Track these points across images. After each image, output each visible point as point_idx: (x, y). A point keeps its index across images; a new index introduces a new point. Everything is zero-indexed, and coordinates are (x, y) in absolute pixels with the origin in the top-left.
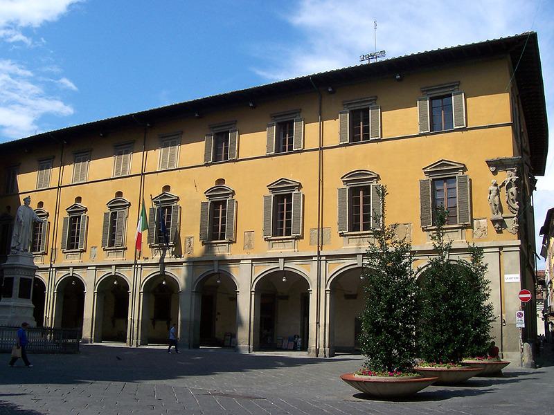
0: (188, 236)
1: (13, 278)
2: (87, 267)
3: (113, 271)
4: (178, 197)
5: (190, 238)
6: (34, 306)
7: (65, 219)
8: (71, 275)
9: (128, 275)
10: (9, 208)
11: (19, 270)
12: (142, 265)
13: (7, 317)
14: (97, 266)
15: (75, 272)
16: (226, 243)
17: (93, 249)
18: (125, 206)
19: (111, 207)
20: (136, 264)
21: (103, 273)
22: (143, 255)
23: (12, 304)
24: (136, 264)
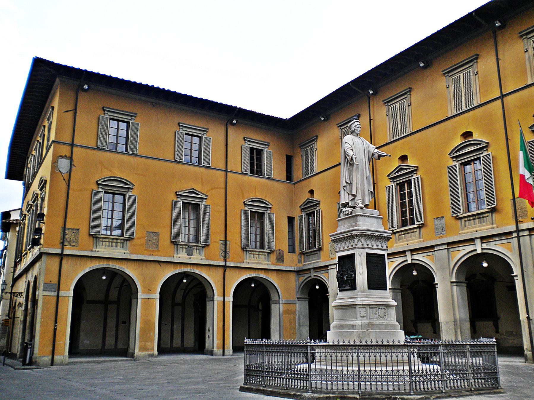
2: (432, 247)
3: (478, 248)
6: (396, 304)
7: (389, 189)
8: (409, 261)
10: (311, 192)
13: (353, 326)
14: (448, 244)
15: (415, 257)
17: (437, 222)
20: (518, 231)
21: (462, 253)
23: (358, 301)
24: (518, 231)
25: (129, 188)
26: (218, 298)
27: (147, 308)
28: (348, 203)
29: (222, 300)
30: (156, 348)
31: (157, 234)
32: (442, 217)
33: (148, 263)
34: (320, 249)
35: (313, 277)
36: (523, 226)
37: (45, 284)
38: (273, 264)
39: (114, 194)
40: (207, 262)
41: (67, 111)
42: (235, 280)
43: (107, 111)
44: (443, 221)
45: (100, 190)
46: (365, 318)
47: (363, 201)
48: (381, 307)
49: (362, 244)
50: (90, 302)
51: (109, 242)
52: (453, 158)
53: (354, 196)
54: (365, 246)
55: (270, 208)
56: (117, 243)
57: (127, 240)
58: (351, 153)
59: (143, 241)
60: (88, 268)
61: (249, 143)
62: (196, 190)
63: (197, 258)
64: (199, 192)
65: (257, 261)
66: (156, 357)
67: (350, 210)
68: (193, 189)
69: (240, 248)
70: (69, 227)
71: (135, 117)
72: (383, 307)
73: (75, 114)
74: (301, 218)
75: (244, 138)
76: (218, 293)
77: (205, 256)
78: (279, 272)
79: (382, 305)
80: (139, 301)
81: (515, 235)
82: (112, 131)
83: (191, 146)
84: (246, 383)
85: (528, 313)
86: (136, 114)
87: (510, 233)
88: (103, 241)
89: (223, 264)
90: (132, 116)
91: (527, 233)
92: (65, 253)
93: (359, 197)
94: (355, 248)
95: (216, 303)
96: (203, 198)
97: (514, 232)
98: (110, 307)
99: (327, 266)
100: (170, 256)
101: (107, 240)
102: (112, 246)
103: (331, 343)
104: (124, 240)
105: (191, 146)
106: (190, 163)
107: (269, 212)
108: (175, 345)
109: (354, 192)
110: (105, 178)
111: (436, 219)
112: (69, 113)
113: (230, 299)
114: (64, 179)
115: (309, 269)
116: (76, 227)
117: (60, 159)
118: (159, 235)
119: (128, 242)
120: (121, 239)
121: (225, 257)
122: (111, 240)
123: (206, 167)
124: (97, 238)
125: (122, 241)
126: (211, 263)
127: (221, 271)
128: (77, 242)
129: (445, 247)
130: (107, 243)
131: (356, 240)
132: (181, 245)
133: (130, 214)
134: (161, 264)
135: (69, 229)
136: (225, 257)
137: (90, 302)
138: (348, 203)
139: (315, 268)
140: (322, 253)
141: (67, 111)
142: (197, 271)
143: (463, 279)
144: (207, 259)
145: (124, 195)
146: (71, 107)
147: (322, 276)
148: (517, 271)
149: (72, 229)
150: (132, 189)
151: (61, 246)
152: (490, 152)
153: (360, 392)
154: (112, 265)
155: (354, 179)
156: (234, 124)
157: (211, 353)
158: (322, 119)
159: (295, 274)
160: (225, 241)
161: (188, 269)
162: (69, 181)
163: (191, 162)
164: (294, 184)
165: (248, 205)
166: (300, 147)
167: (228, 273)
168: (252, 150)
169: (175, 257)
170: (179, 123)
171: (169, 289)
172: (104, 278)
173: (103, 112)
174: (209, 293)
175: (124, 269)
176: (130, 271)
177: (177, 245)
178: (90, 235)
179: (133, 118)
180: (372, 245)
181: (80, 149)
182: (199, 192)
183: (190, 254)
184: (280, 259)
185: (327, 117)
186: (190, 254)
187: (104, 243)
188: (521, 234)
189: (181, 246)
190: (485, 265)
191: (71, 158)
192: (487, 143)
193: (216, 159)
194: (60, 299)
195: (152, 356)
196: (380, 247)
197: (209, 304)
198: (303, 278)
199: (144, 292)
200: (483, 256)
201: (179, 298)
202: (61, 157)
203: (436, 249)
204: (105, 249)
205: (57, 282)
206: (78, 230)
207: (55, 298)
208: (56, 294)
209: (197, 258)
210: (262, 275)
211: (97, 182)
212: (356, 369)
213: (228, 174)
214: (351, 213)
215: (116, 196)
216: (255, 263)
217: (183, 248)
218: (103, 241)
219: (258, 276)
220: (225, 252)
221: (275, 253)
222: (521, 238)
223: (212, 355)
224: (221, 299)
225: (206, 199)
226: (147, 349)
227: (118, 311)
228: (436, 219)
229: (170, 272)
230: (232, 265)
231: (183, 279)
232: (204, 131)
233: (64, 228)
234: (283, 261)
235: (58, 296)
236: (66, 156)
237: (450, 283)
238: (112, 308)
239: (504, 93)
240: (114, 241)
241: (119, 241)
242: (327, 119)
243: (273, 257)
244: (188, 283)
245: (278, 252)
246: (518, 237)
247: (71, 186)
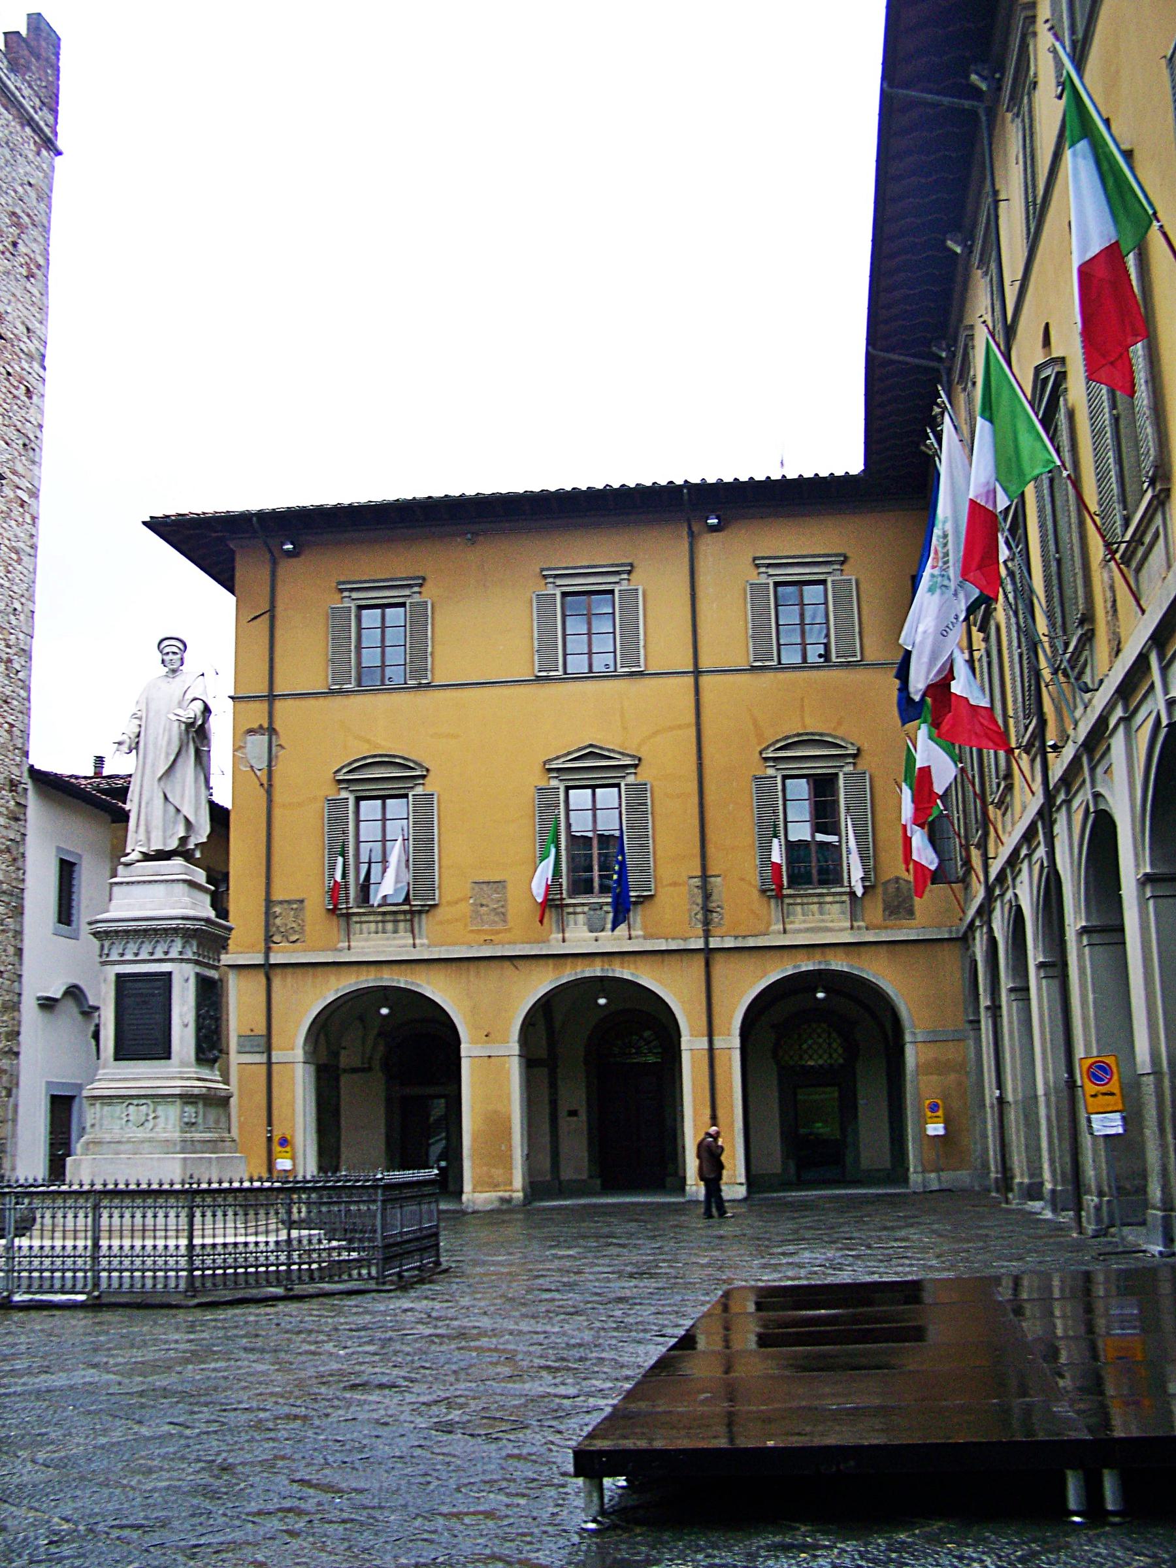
26: (691, 1044)
29: (706, 1046)
37: (240, 1036)
41: (255, 618)
42: (743, 988)
45: (344, 794)
48: (135, 1102)
51: (377, 922)
55: (855, 756)
56: (396, 921)
57: (420, 912)
59: (465, 908)
60: (332, 992)
61: (771, 571)
62: (601, 748)
64: (609, 750)
65: (821, 926)
68: (591, 746)
69: (755, 894)
70: (281, 898)
71: (421, 585)
73: (273, 619)
76: (692, 1028)
77: (644, 928)
78: (898, 948)
79: (139, 1097)
82: (371, 638)
86: (424, 579)
88: (361, 922)
89: (699, 944)
92: (272, 961)
100: (537, 942)
101: (371, 918)
102: (384, 932)
104: (412, 912)
106: (591, 675)
107: (850, 768)
110: (350, 764)
112: (259, 620)
113: (730, 1041)
114: (262, 785)
116: (298, 897)
117: (249, 738)
118: (505, 887)
119: (424, 916)
120: (405, 912)
122: (380, 918)
123: (632, 674)
125: (408, 917)
127: (698, 963)
128: (302, 932)
130: (373, 926)
132: (568, 905)
133: (421, 846)
134: (520, 963)
135: (281, 902)
136: (706, 923)
141: (255, 618)
142: (624, 972)
149: (289, 902)
150: (424, 777)
151: (262, 945)
156: (714, 529)
160: (705, 877)
161: (595, 970)
162: (270, 785)
163: (591, 671)
167: (720, 968)
169: (553, 942)
171: (545, 1028)
175: (418, 985)
176: (436, 989)
179: (416, 589)
181: (290, 702)
182: (609, 750)
187: (365, 926)
189: (571, 910)
191: (272, 731)
193: (665, 643)
194: (275, 1068)
195: (508, 1201)
196: (159, 955)
199: (473, 1042)
202: (251, 731)
204: (366, 940)
205: (264, 1032)
206: (302, 901)
207: (264, 1067)
208: (263, 1058)
210: (839, 964)
212: (183, 1242)
215: (388, 801)
216: (807, 930)
217: (575, 913)
218: (361, 922)
219: (822, 967)
220: (707, 911)
221: (880, 890)
225: (636, 766)
226: (495, 1186)
229: (542, 983)
230: (729, 943)
232: (618, 573)
233: (269, 902)
235: (269, 1063)
236: (261, 727)
240: (388, 918)
241: (401, 917)
245: (891, 889)
247: (278, 797)
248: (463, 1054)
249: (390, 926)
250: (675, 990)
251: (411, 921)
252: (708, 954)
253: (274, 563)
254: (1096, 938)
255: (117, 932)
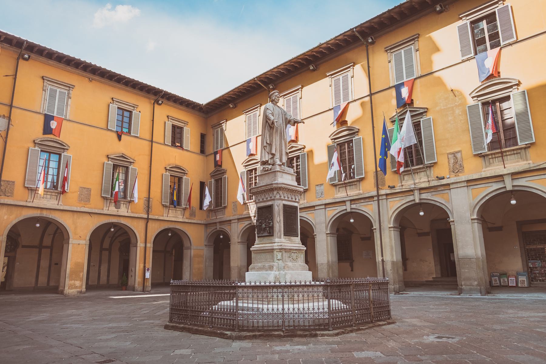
0: (452, 151)
1: (272, 205)
2: (314, 207)
3: (348, 207)
4: (427, 109)
5: (454, 154)
6: (305, 248)
9: (369, 209)
11: (281, 192)
12: (387, 195)
16: (521, 149)
17: (318, 188)
18: (354, 133)
19: (335, 139)
20: (378, 196)
22: (388, 183)
24: (378, 196)
25: (64, 149)
26: (140, 245)
27: (77, 253)
28: (268, 161)
30: (84, 287)
31: (89, 190)
32: (322, 185)
33: (79, 213)
34: (225, 207)
35: (218, 229)
36: (382, 192)
38: (187, 218)
39: (50, 153)
40: (132, 215)
42: (154, 229)
43: (46, 80)
44: (322, 187)
45: (37, 148)
46: (281, 261)
47: (281, 160)
49: (280, 196)
50: (23, 247)
52: (332, 139)
53: (273, 155)
54: (282, 198)
58: (272, 118)
63: (123, 210)
65: (175, 216)
66: (84, 293)
67: (270, 167)
71: (73, 88)
72: (295, 251)
74: (211, 183)
75: (168, 116)
79: (296, 250)
80: (70, 246)
81: (376, 198)
83: (123, 118)
84: (171, 321)
85: (382, 256)
87: (373, 197)
89: (146, 216)
90: (69, 87)
91: (384, 197)
93: (278, 156)
94: (274, 200)
95: (138, 249)
96: (131, 162)
97: (376, 196)
98: (43, 250)
99: (230, 220)
103: (248, 284)
104: (58, 193)
105: (123, 118)
108: (101, 283)
109: (273, 152)
111: (317, 185)
113: (150, 245)
115: (216, 223)
121: (148, 211)
124: (32, 190)
126: (136, 215)
129: (323, 207)
131: (275, 192)
135: (4, 181)
137: (23, 247)
138: (268, 161)
139: (220, 222)
140: (226, 210)
142: (123, 221)
143: (335, 232)
144: (132, 212)
145: (60, 155)
146: (11, 72)
147: (226, 228)
148: (376, 226)
149: (8, 181)
150: (67, 149)
152: (360, 136)
153: (284, 329)
154: (45, 214)
155: (274, 140)
156: (160, 104)
157: (133, 289)
158: (231, 106)
159: (203, 227)
160: (149, 198)
162: (6, 137)
164: (206, 156)
165: (169, 170)
166: (212, 127)
167: (150, 224)
168: (174, 127)
170: (112, 98)
172: (38, 225)
173: (42, 81)
174: (133, 240)
177: (107, 199)
178: (25, 187)
180: (288, 198)
183: (117, 207)
184: (193, 215)
185: (235, 105)
186: (117, 207)
188: (380, 198)
190: (352, 221)
191: (9, 118)
192: (359, 129)
197: (132, 249)
198: (211, 230)
200: (352, 214)
201: (106, 245)
203: (316, 208)
206: (14, 182)
209: (123, 210)
211: (34, 141)
213: (153, 144)
214: (270, 170)
222: (380, 201)
223: (134, 291)
224: (143, 245)
227: (51, 255)
228: (317, 185)
231: (111, 228)
234: (195, 216)
236: (4, 116)
237: (325, 235)
238: (45, 253)
239: (372, 92)
240: (48, 193)
242: (235, 107)
243: (187, 213)
244: (115, 232)
246: (378, 200)
248: (70, 242)
249: (49, 196)
250: (138, 228)
251: (57, 196)
252: (148, 219)
253: (18, 59)
254: (395, 229)
255: (289, 189)
